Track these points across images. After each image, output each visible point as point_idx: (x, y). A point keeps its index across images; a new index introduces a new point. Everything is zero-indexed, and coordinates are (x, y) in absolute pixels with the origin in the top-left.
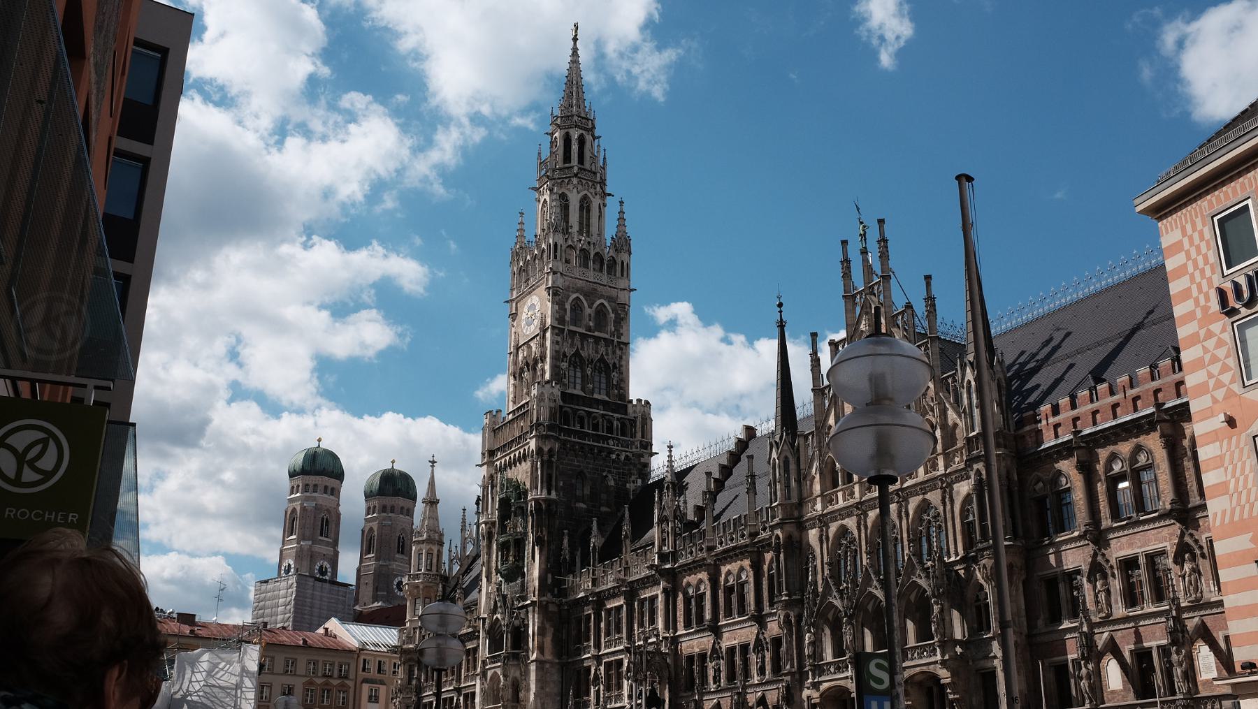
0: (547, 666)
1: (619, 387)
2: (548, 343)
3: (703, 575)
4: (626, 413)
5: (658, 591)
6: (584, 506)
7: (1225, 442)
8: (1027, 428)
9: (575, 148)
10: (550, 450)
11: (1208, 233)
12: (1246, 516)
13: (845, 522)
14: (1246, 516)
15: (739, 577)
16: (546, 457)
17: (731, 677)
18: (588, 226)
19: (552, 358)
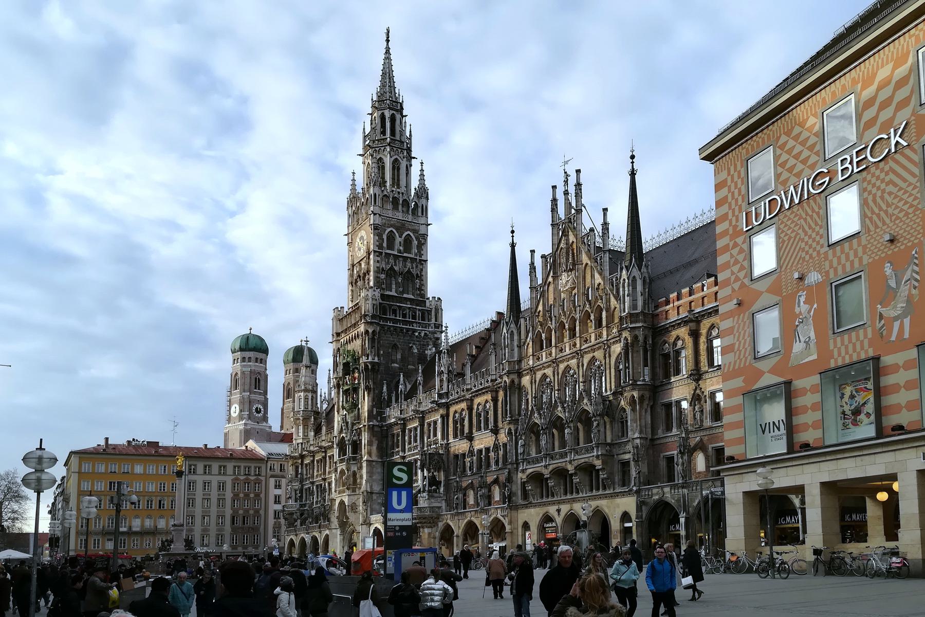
1: (420, 289)
3: (463, 405)
5: (437, 417)
8: (660, 310)
13: (545, 371)
19: (375, 272)
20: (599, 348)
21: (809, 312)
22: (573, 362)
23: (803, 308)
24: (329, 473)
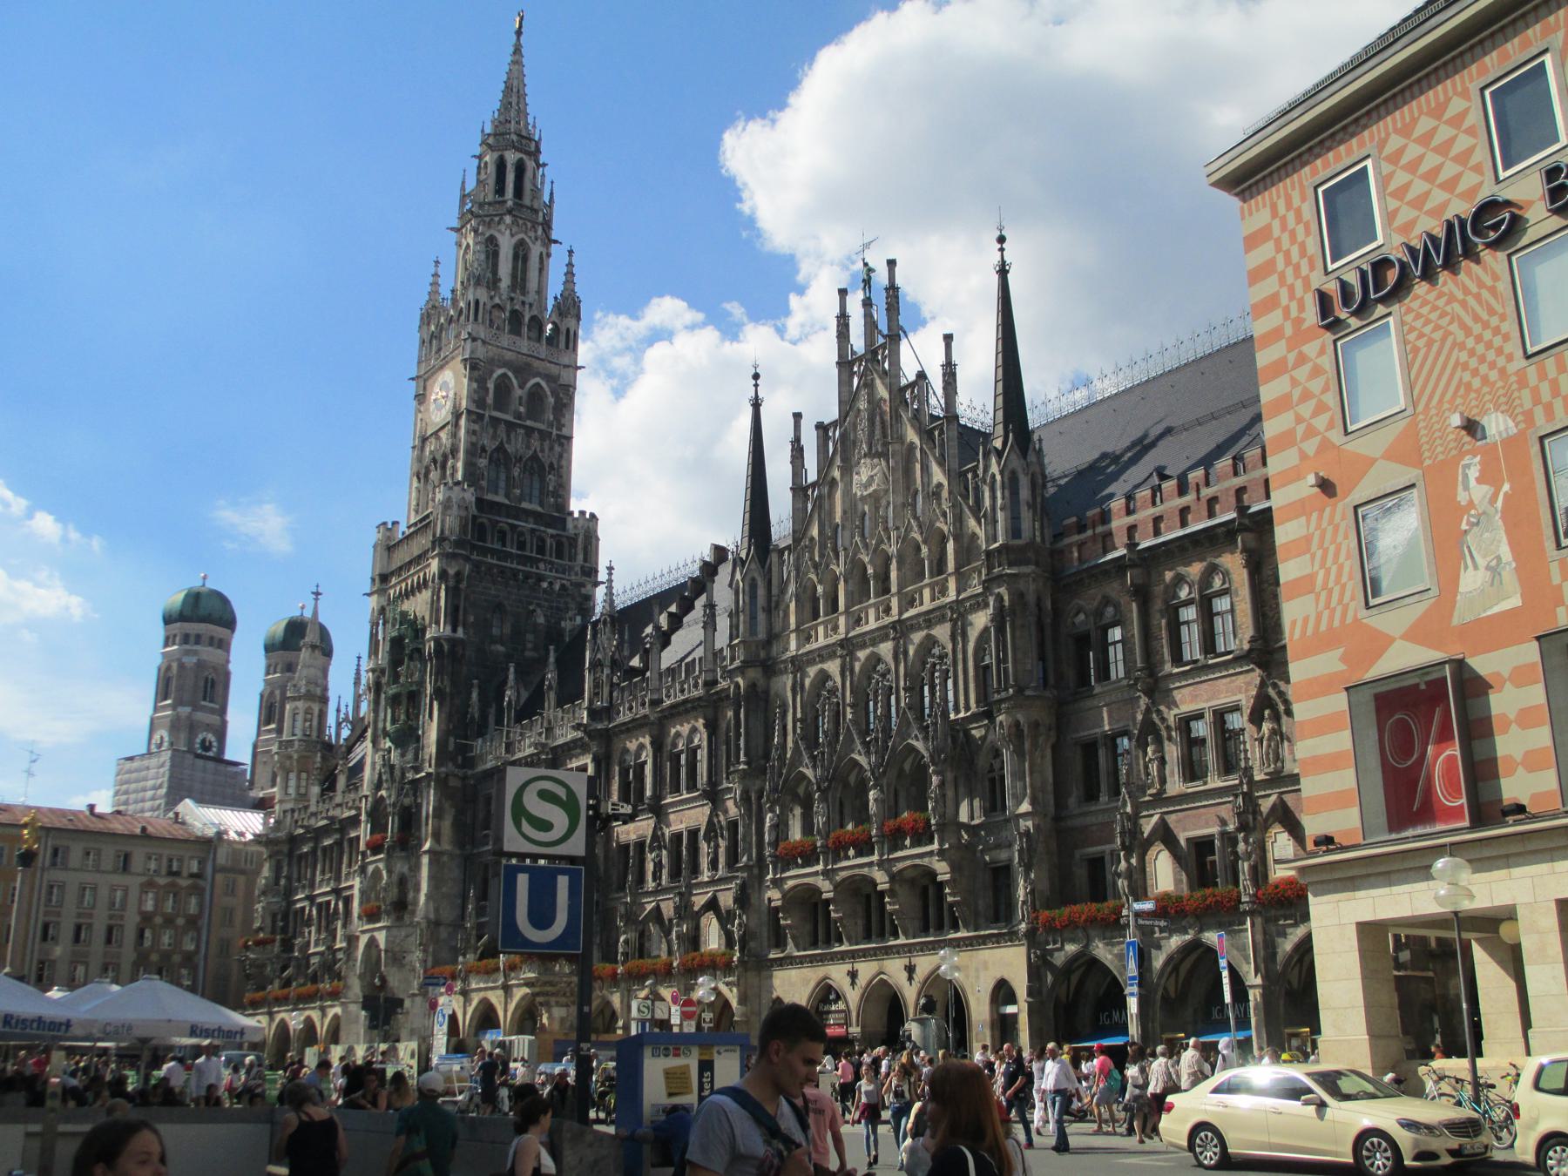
0: (445, 858)
2: (462, 432)
4: (564, 528)
6: (501, 648)
7: (1315, 515)
9: (510, 178)
10: (458, 574)
11: (1308, 211)
12: (1336, 624)
13: (825, 666)
14: (1336, 624)
15: (690, 740)
16: (452, 583)
17: (675, 874)
18: (524, 280)
19: (469, 453)
20: (942, 619)
24: (348, 874)
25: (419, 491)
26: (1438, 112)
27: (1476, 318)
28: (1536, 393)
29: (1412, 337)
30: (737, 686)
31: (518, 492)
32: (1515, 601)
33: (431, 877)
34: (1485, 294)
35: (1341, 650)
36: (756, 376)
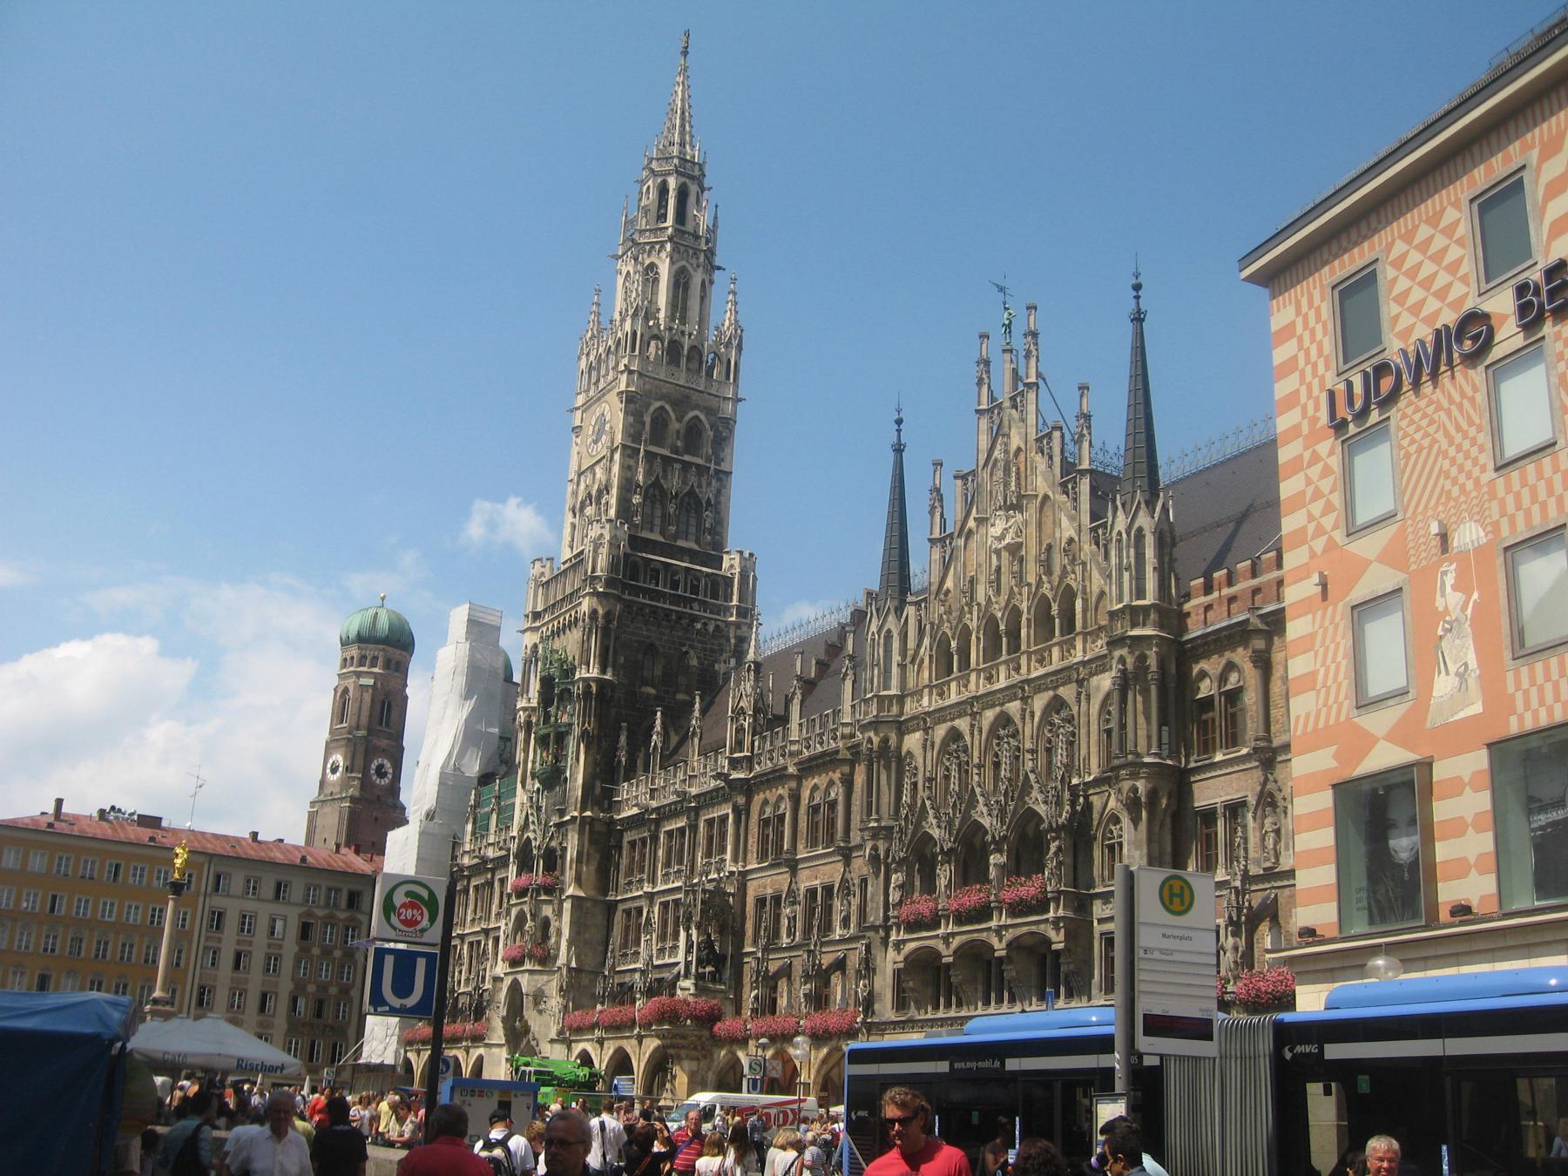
0: (589, 904)
2: (616, 469)
5: (727, 809)
6: (651, 691)
7: (1319, 614)
11: (1326, 310)
12: (1332, 722)
14: (1332, 722)
15: (827, 792)
17: (807, 931)
18: (685, 309)
19: (620, 488)
21: (1464, 608)
22: (1014, 707)
23: (1450, 599)
24: (498, 914)
25: (574, 526)
26: (1434, 221)
27: (1458, 428)
28: (1502, 504)
29: (1405, 442)
30: (870, 741)
31: (673, 529)
32: (1477, 708)
33: (574, 923)
34: (1466, 404)
35: (1332, 750)
36: (899, 422)
